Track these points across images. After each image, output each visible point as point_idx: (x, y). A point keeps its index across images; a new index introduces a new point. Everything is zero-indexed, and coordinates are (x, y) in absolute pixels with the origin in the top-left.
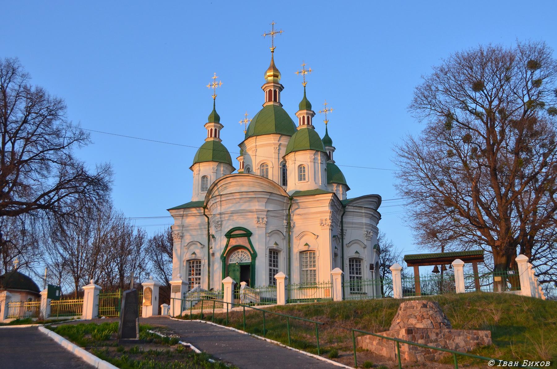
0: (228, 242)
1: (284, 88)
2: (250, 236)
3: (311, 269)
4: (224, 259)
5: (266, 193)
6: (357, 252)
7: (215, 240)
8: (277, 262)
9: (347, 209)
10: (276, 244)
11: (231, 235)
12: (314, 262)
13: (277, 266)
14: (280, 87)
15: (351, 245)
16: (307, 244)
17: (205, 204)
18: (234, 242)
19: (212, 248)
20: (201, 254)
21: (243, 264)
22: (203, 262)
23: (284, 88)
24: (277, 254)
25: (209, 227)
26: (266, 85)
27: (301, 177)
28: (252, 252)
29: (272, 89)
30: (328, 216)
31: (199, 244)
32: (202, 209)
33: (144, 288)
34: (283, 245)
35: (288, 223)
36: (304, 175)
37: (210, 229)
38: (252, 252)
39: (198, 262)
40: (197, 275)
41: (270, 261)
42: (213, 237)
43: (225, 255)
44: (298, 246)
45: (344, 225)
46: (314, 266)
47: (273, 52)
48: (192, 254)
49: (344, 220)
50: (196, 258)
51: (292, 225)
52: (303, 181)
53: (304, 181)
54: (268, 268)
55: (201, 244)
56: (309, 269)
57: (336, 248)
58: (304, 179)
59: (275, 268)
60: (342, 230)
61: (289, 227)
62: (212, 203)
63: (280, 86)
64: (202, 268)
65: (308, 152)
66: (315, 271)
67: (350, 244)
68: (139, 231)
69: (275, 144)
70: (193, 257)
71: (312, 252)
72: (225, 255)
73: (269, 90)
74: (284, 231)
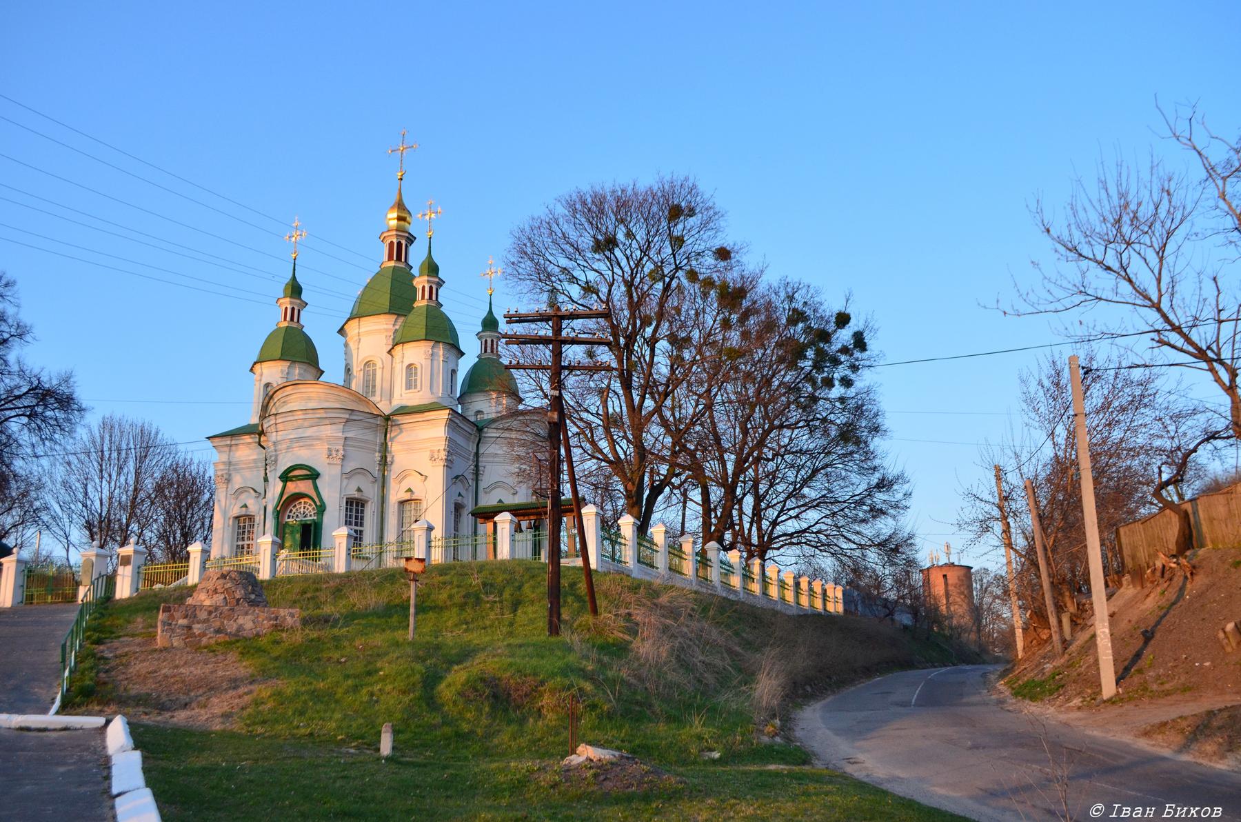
0: (284, 487)
1: (415, 238)
2: (317, 478)
4: (278, 514)
5: (343, 411)
8: (362, 518)
9: (487, 433)
10: (359, 490)
13: (362, 525)
14: (408, 237)
15: (491, 490)
16: (409, 490)
17: (260, 429)
18: (293, 488)
20: (254, 507)
22: (257, 519)
23: (415, 238)
24: (363, 506)
27: (410, 385)
29: (395, 241)
30: (441, 445)
31: (252, 491)
32: (257, 436)
34: (371, 492)
35: (382, 457)
36: (416, 380)
38: (318, 503)
39: (251, 518)
44: (396, 493)
45: (480, 459)
47: (401, 179)
49: (481, 451)
50: (248, 513)
51: (388, 460)
53: (416, 390)
57: (460, 495)
60: (477, 466)
61: (384, 462)
63: (407, 235)
65: (423, 343)
69: (387, 330)
70: (243, 511)
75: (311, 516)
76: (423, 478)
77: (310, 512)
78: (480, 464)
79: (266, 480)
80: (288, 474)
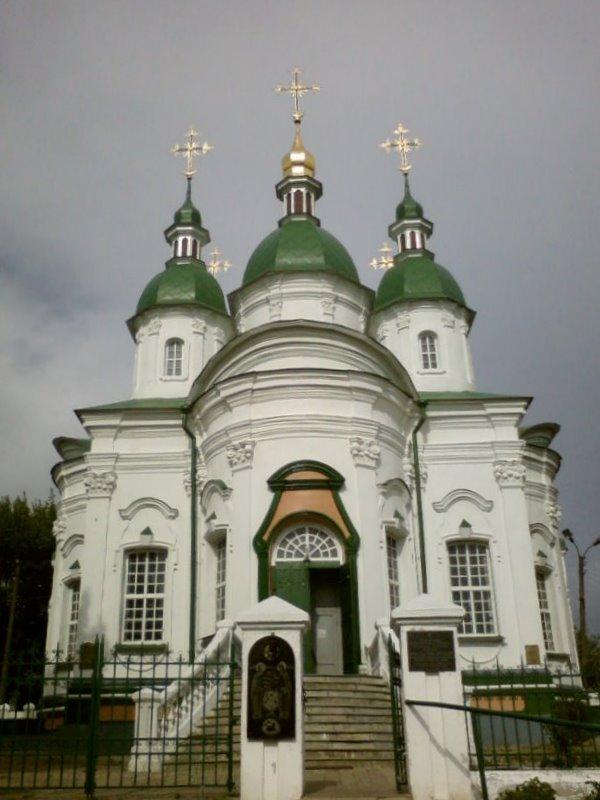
3: (476, 588)
4: (262, 547)
7: (226, 497)
10: (397, 515)
11: (287, 482)
16: (465, 524)
18: (297, 502)
20: (173, 535)
21: (313, 566)
25: (194, 463)
27: (430, 361)
28: (347, 534)
38: (347, 534)
39: (159, 553)
40: (151, 590)
42: (224, 488)
43: (265, 537)
46: (485, 582)
52: (431, 370)
56: (470, 588)
62: (224, 394)
64: (168, 573)
72: (265, 537)
75: (326, 554)
77: (323, 547)
80: (291, 472)
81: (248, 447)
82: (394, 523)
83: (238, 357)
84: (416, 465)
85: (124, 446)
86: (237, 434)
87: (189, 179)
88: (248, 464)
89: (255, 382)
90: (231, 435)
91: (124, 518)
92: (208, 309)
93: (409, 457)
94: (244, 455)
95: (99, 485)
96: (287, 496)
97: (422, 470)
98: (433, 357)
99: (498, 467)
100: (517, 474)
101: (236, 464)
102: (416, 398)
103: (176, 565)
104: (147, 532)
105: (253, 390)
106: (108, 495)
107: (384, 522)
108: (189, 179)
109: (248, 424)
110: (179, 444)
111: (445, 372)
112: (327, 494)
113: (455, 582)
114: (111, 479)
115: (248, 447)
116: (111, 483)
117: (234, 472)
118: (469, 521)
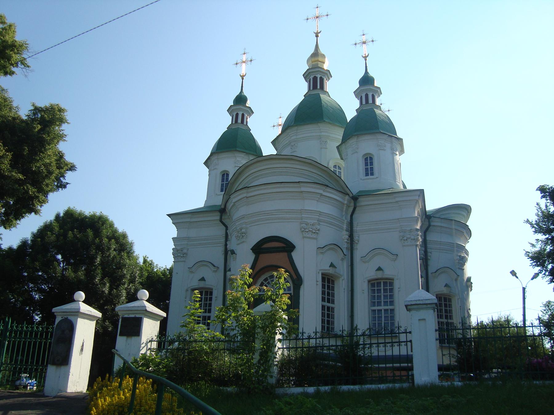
2: (292, 251)
3: (386, 307)
6: (446, 285)
8: (333, 296)
10: (332, 265)
12: (391, 296)
13: (333, 302)
16: (379, 269)
19: (230, 270)
22: (215, 294)
24: (333, 282)
26: (310, 71)
28: (295, 277)
32: (219, 214)
33: (58, 320)
37: (228, 243)
38: (295, 277)
41: (323, 293)
42: (233, 252)
45: (428, 245)
46: (392, 303)
48: (199, 280)
52: (370, 177)
53: (372, 177)
54: (320, 303)
55: (214, 266)
56: (383, 307)
58: (372, 174)
59: (330, 305)
62: (234, 200)
64: (213, 302)
66: (392, 310)
67: (437, 273)
68: (145, 261)
71: (388, 281)
73: (313, 76)
74: (345, 245)
76: (395, 257)
78: (429, 250)
79: (228, 253)
81: (243, 230)
82: (329, 270)
83: (241, 180)
84: (351, 236)
85: (193, 233)
86: (239, 223)
87: (242, 77)
88: (244, 240)
89: (247, 193)
90: (237, 224)
91: (192, 272)
92: (244, 152)
93: (346, 231)
94: (242, 235)
95: (179, 254)
96: (262, 256)
97: (356, 238)
98: (372, 169)
99: (402, 234)
100: (413, 237)
101: (238, 240)
102: (351, 195)
103: (216, 297)
104: (203, 279)
105: (247, 198)
106: (184, 260)
107: (320, 270)
108: (242, 77)
109: (243, 217)
110: (219, 231)
111: (377, 178)
112: (283, 256)
113: (373, 304)
114: (185, 251)
115: (243, 230)
116: (185, 254)
117: (238, 244)
118: (382, 267)
